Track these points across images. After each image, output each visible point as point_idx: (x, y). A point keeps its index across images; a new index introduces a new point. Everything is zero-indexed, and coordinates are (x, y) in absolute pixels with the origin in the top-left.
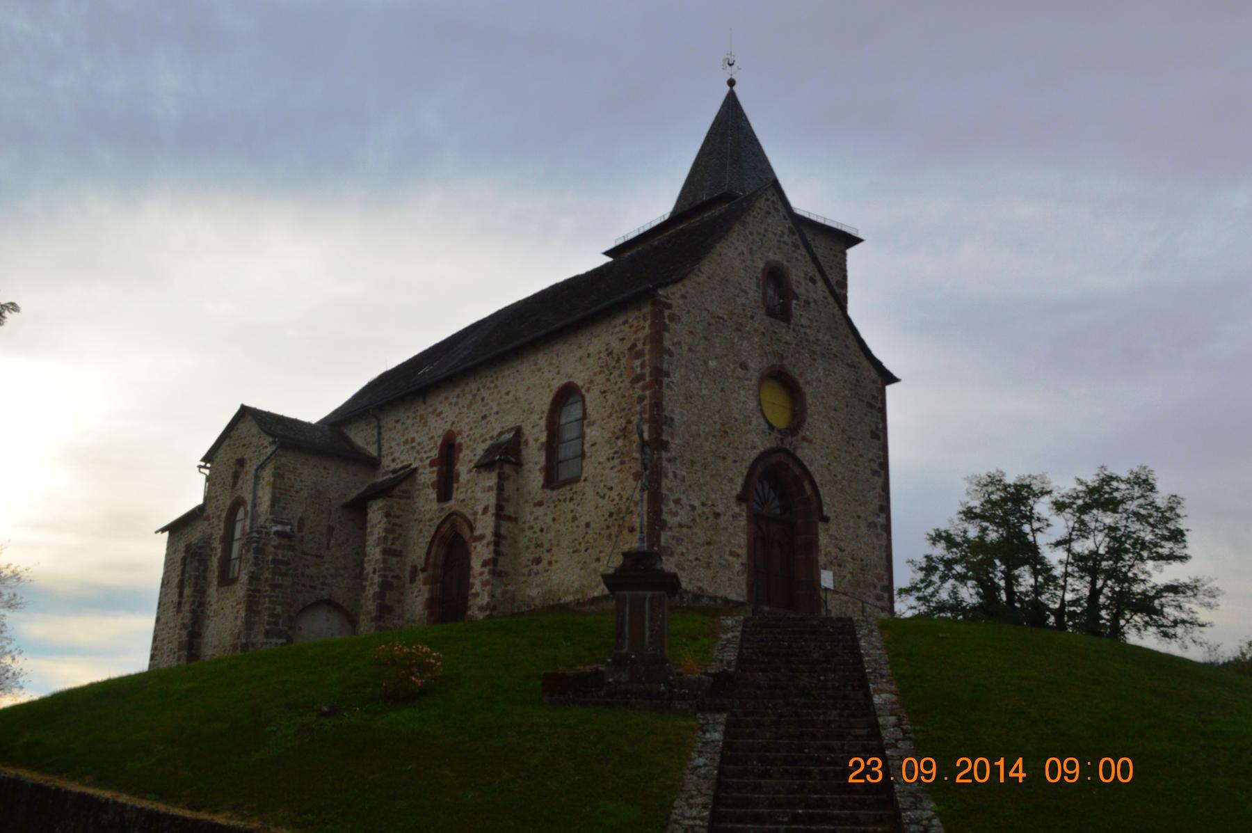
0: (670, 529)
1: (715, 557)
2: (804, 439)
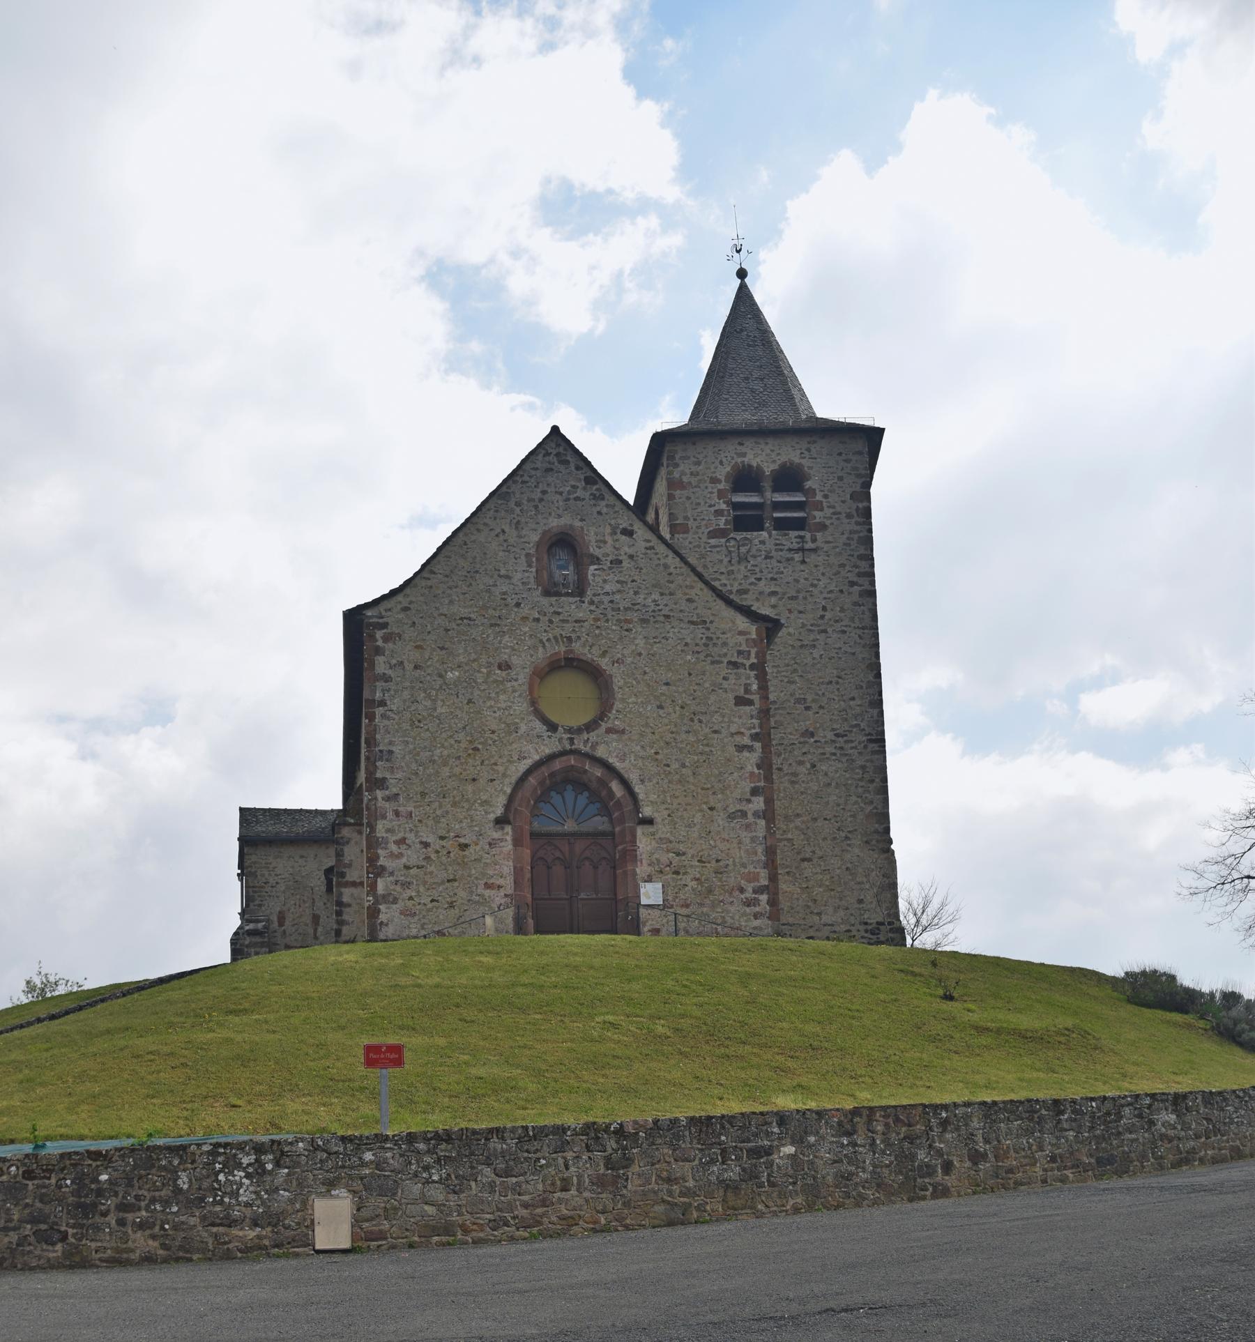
0: (392, 874)
1: (462, 894)
2: (609, 731)
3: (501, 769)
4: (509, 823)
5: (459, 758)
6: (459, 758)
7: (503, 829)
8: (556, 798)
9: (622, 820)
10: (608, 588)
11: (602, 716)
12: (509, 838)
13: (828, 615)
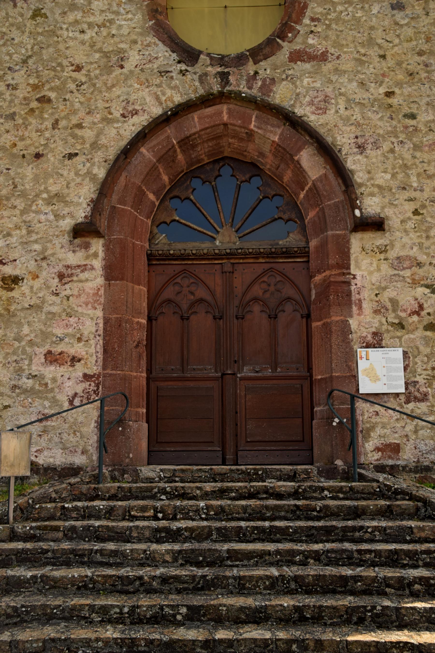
2: (296, 57)
3: (88, 134)
4: (98, 234)
5: (12, 116)
6: (12, 116)
7: (87, 246)
9: (321, 226)
11: (284, 31)
12: (98, 264)
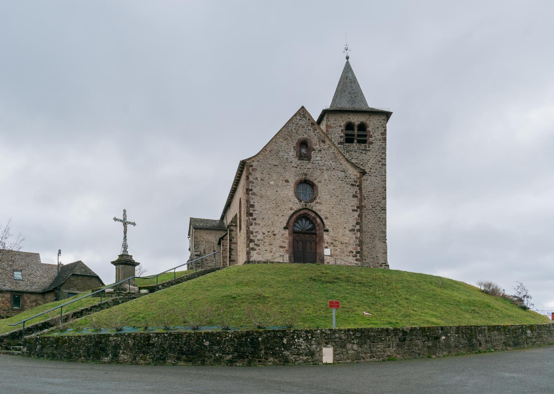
2: (317, 203)
3: (286, 212)
8: (300, 222)
9: (319, 230)
10: (317, 158)
11: (315, 198)
13: (372, 171)
